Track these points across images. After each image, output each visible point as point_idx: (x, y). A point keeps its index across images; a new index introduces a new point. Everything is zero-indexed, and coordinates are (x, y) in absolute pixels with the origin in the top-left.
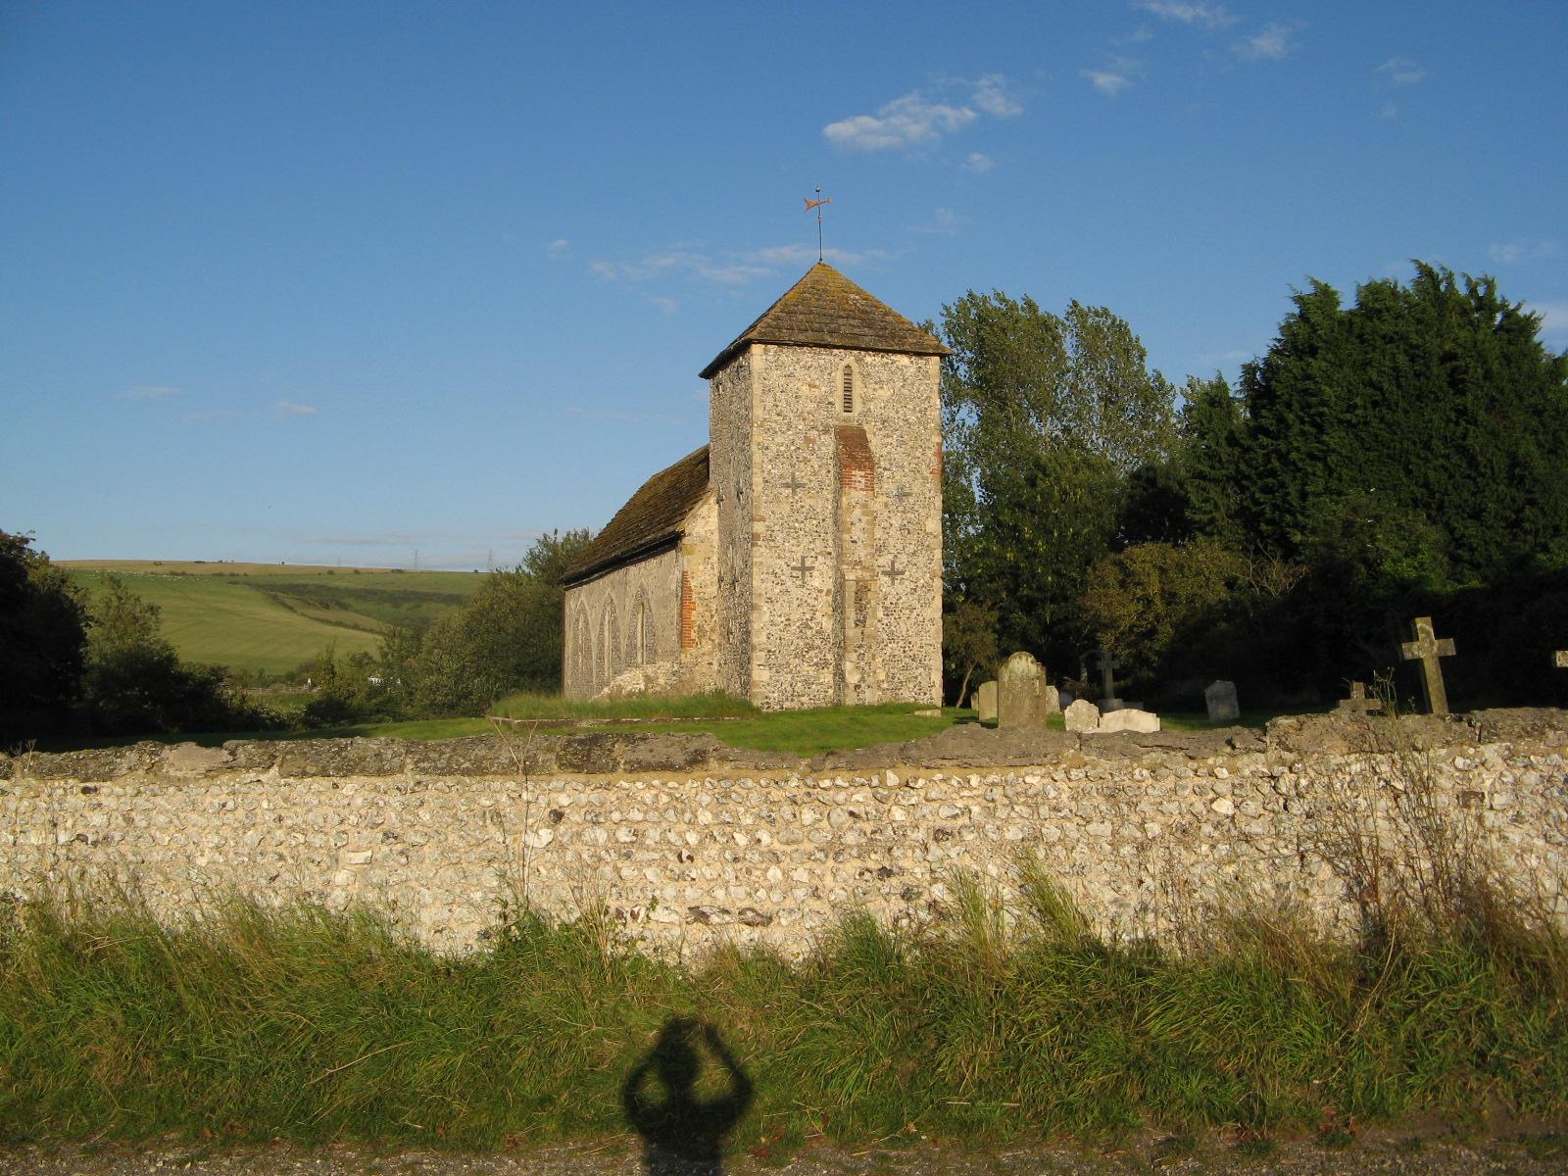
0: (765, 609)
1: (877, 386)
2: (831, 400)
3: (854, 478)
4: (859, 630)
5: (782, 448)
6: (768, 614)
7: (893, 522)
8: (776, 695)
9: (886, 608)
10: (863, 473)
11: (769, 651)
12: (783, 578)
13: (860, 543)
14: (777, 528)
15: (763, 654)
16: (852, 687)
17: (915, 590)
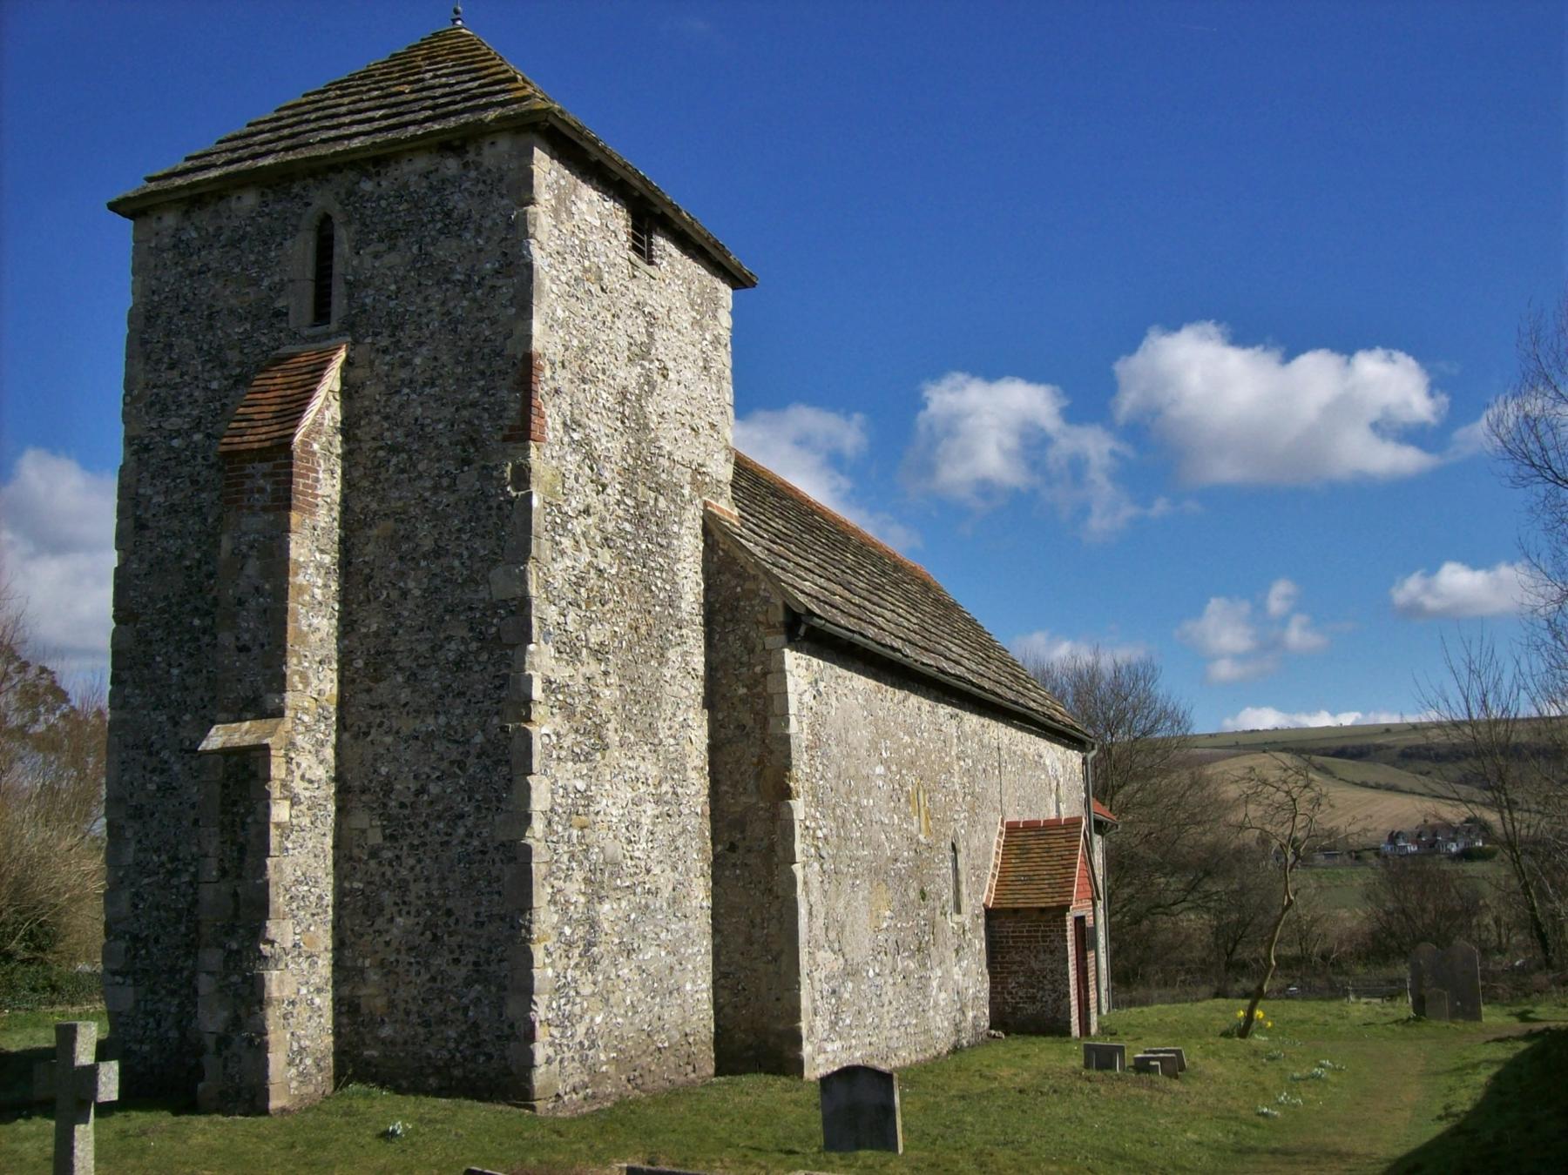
0: (129, 834)
1: (382, 247)
2: (280, 304)
3: (248, 484)
4: (224, 887)
5: (176, 443)
6: (133, 846)
7: (411, 584)
8: (146, 1048)
9: (390, 818)
10: (266, 467)
11: (135, 938)
12: (165, 754)
13: (256, 650)
14: (159, 633)
15: (123, 945)
16: (210, 1042)
17: (461, 765)
